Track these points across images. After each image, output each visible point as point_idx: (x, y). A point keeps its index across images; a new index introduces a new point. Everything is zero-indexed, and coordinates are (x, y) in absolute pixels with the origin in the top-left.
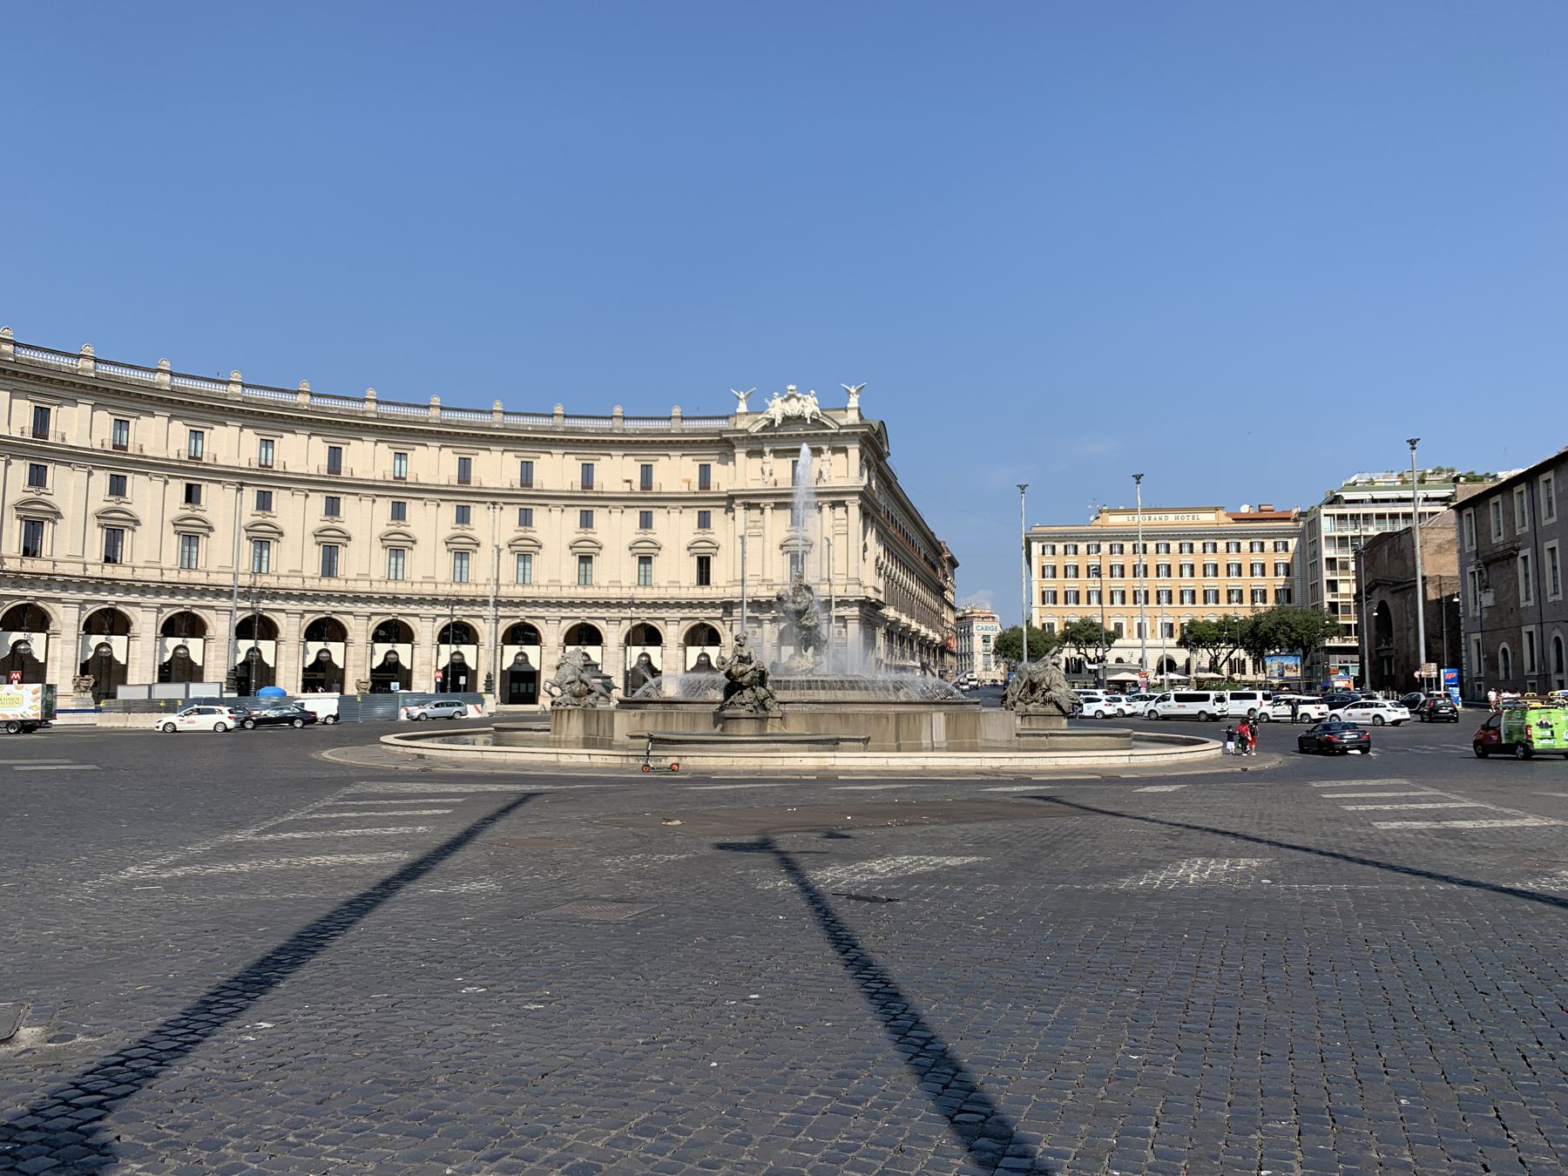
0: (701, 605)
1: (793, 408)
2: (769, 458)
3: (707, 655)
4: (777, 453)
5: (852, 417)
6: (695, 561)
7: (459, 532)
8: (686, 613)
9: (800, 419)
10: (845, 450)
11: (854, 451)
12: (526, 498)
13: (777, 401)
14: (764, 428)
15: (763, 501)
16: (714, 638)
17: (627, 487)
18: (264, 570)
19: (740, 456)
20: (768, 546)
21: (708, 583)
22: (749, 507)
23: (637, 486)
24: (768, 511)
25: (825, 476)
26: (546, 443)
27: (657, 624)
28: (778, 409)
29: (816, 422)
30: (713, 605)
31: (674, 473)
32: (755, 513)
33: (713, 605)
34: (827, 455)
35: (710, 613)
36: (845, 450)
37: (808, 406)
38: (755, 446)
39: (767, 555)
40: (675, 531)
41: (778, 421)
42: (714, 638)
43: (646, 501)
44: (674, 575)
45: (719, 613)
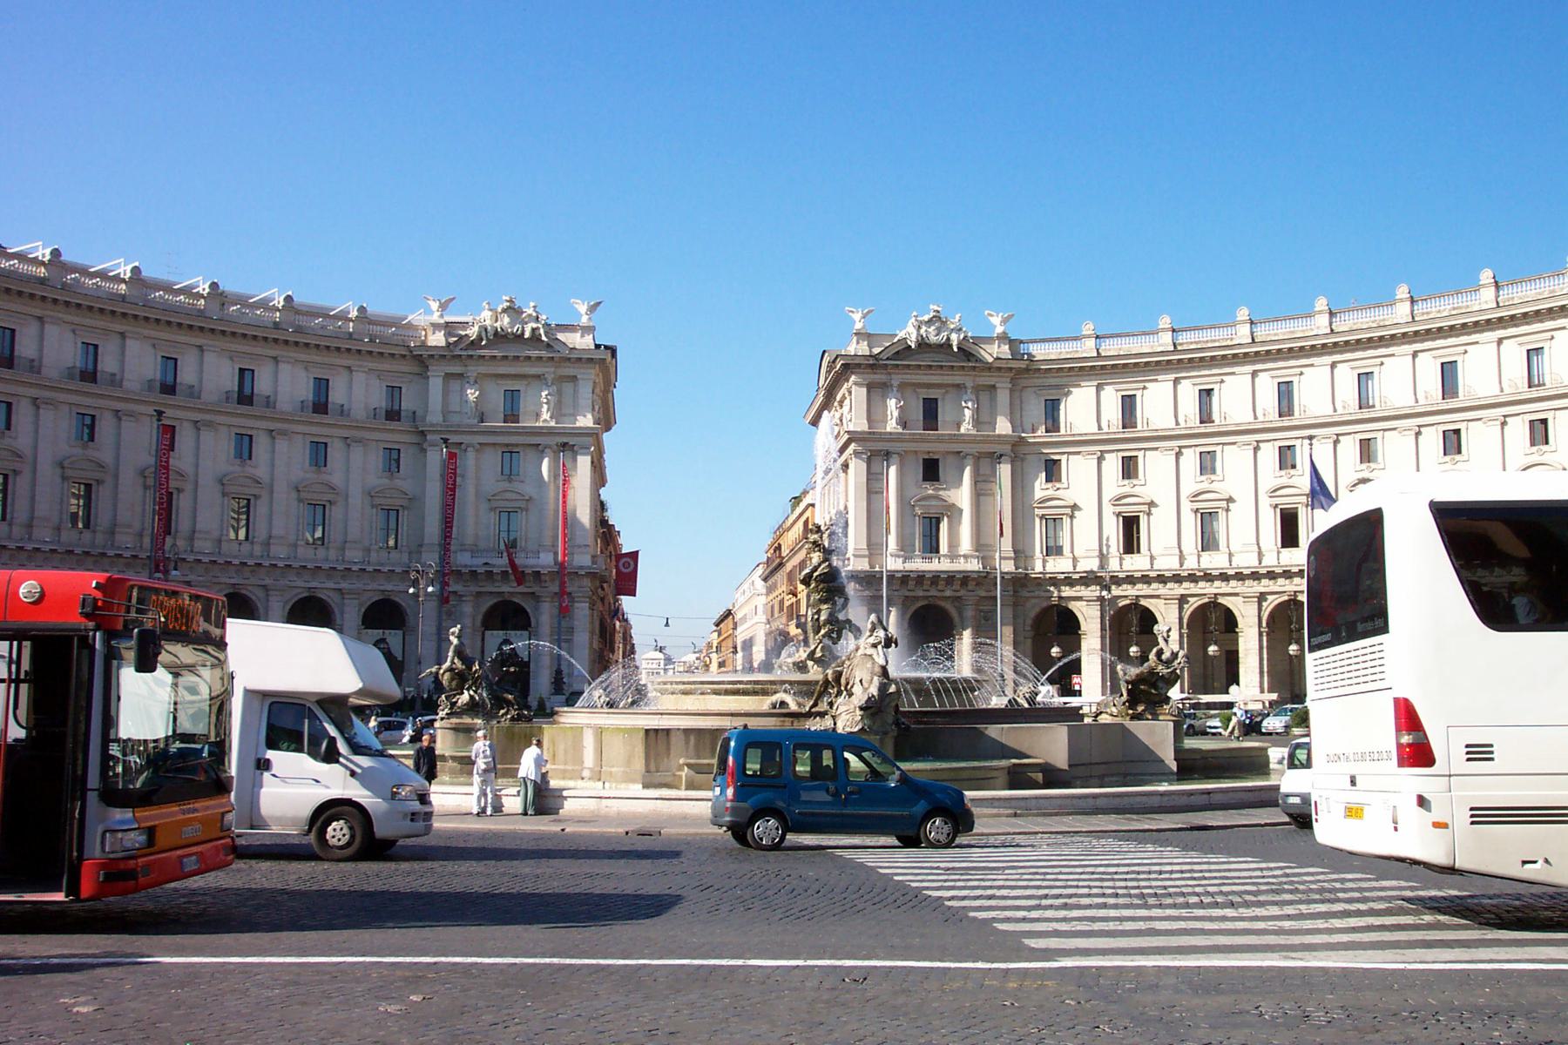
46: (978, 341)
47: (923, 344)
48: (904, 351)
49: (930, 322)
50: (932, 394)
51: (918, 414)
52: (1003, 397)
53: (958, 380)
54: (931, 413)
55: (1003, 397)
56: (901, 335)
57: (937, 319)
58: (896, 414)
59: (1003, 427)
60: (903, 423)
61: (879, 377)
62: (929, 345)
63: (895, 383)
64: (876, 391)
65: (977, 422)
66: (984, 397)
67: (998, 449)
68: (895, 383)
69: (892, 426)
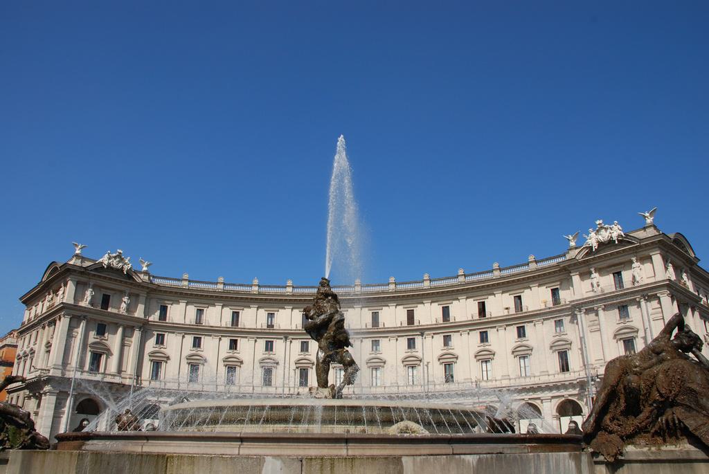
0: (564, 386)
1: (604, 236)
2: (595, 275)
3: (575, 423)
4: (601, 271)
5: (651, 232)
6: (556, 355)
7: (409, 354)
8: (555, 393)
9: (610, 242)
10: (649, 259)
11: (657, 258)
12: (447, 328)
13: (593, 234)
14: (587, 254)
15: (595, 306)
16: (577, 411)
17: (506, 312)
18: (374, 384)
19: (576, 278)
20: (605, 337)
21: (568, 370)
22: (588, 312)
23: (512, 311)
24: (601, 312)
25: (638, 278)
26: (454, 293)
27: (537, 403)
28: (593, 240)
29: (622, 242)
30: (573, 386)
31: (536, 298)
32: (592, 316)
33: (573, 386)
34: (636, 264)
35: (572, 391)
36: (649, 259)
37: (616, 232)
38: (584, 267)
39: (605, 343)
40: (540, 335)
41: (595, 246)
42: (577, 411)
43: (520, 321)
44: (544, 367)
45: (576, 391)
46: (136, 272)
47: (109, 266)
48: (100, 268)
49: (115, 257)
50: (108, 292)
51: (99, 300)
52: (142, 299)
53: (122, 288)
54: (106, 302)
55: (142, 299)
56: (101, 260)
57: (119, 256)
58: (89, 299)
59: (139, 313)
60: (92, 303)
61: (83, 279)
62: (112, 268)
63: (92, 283)
64: (81, 286)
65: (128, 310)
66: (133, 298)
67: (135, 324)
68: (92, 283)
69: (84, 303)
